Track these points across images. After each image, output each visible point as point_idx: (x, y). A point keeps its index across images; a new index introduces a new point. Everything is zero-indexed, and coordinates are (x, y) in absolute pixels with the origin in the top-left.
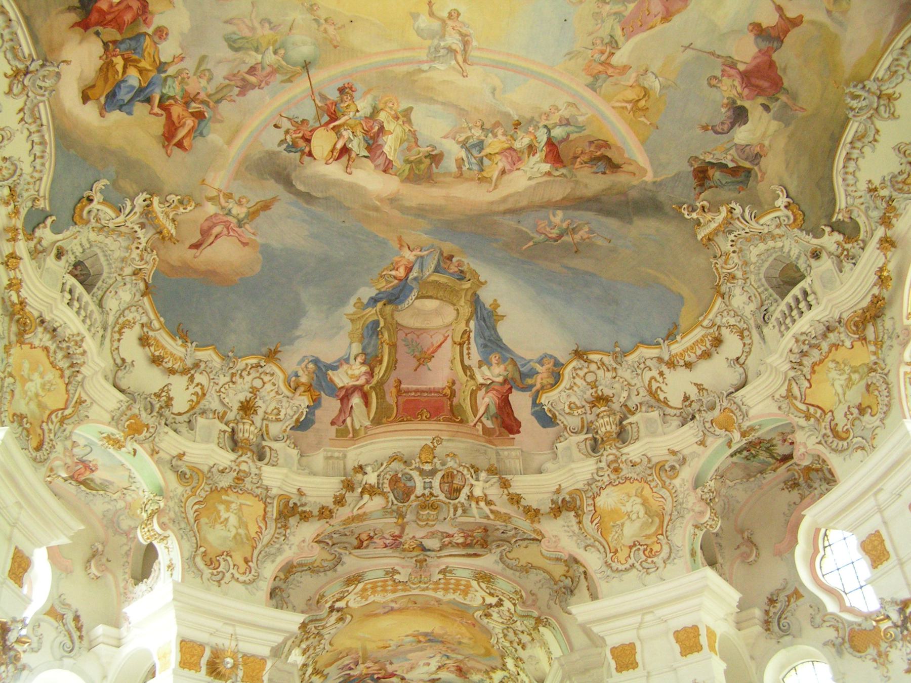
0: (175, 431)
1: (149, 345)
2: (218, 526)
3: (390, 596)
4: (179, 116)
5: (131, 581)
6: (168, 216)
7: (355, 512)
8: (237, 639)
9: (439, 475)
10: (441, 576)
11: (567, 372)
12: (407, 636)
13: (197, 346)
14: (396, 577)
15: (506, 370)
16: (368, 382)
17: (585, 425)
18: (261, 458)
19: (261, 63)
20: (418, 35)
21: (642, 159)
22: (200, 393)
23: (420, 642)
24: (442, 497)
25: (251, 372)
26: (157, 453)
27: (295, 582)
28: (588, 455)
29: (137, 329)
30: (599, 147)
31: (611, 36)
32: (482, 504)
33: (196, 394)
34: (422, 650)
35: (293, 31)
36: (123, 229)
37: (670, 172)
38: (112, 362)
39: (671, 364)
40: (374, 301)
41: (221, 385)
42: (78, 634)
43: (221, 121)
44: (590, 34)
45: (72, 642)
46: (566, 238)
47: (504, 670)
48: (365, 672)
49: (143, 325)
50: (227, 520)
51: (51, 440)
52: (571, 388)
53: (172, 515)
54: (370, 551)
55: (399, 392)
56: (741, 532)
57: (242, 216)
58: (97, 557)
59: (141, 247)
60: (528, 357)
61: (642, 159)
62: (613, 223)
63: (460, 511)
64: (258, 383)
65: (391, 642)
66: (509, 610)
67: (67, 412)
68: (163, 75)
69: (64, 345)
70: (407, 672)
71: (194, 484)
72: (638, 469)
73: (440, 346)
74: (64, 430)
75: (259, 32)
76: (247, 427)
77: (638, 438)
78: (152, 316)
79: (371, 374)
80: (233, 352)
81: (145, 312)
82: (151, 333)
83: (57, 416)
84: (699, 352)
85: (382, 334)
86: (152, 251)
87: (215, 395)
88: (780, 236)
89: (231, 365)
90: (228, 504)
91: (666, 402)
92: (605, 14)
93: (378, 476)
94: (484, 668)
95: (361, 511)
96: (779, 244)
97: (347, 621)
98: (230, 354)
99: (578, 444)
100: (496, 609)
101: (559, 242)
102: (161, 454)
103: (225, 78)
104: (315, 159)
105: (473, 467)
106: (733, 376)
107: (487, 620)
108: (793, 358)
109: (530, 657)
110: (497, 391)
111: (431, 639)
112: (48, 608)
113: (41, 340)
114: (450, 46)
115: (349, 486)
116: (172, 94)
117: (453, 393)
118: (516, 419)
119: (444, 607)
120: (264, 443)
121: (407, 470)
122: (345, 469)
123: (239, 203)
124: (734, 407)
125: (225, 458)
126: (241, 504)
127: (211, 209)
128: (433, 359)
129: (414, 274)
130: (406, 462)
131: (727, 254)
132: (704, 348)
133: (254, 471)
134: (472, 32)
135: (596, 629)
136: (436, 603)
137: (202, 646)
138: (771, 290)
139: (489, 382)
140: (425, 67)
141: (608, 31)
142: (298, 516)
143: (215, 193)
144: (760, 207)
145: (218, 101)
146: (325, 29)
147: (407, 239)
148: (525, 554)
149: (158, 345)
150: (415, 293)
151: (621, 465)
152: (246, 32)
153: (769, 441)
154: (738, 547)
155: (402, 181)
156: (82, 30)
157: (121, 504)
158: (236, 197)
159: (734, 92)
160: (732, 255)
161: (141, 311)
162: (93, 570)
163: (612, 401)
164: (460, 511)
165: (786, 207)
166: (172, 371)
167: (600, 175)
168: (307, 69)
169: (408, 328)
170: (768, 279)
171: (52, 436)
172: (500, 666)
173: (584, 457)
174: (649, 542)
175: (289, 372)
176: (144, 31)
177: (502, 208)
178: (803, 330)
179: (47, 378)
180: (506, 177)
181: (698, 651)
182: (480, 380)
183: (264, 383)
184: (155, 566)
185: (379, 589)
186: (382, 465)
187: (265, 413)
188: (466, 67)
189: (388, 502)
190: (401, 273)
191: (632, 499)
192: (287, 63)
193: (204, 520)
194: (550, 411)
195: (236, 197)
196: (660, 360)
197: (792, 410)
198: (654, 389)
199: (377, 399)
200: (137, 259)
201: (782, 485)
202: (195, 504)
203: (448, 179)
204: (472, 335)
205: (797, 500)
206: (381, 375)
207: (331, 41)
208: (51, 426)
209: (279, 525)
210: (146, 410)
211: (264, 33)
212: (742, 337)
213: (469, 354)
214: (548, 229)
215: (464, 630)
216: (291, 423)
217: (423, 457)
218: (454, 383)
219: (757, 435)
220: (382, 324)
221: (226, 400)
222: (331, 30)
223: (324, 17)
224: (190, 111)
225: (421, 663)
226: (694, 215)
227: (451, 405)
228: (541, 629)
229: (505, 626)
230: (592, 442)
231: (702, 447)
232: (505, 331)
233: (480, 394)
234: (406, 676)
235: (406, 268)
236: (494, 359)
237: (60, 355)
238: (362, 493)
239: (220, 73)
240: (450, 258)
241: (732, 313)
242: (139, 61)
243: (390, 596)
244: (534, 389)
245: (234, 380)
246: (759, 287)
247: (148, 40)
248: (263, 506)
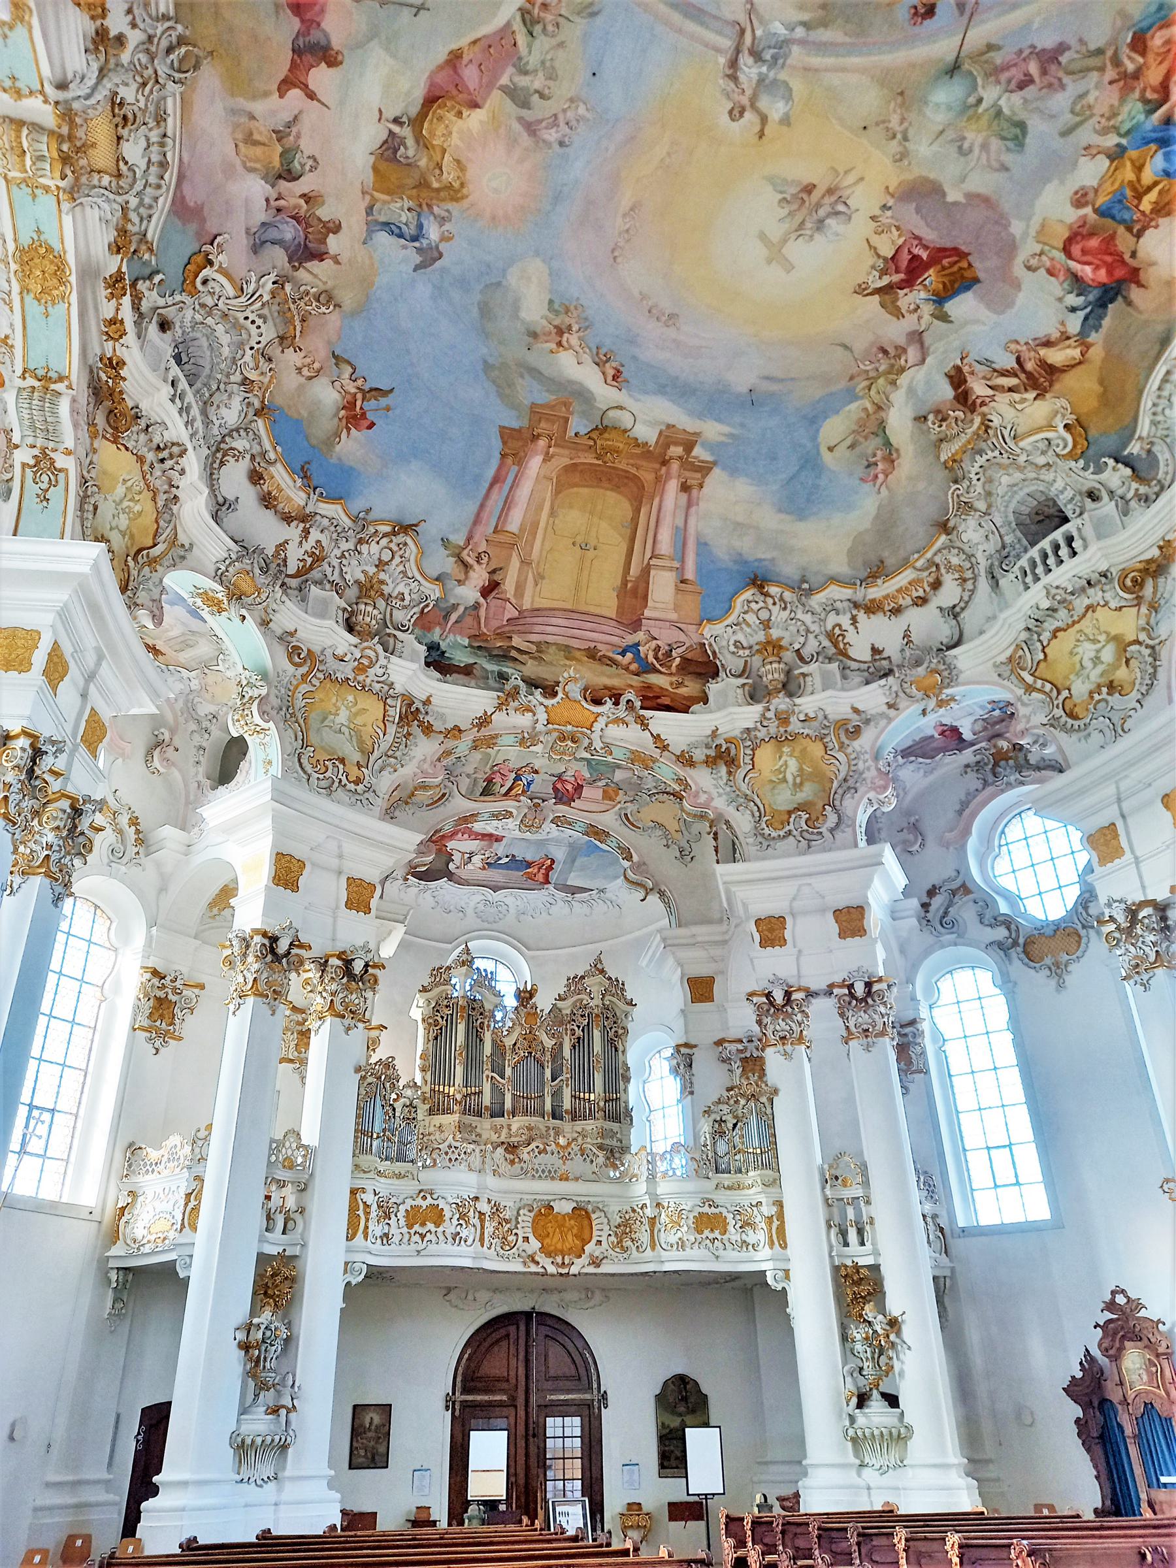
4: (1161, 63)
19: (1007, 91)
20: (791, 90)
31: (531, 34)
35: (941, 128)
43: (1122, 13)
44: (561, 45)
68: (1124, 141)
75: (980, 140)
92: (540, 74)
103: (1063, 87)
114: (756, 62)
116: (1139, 105)
134: (721, 81)
140: (800, 32)
141: (537, 44)
145: (1100, 52)
146: (901, 123)
152: (995, 144)
156: (1142, 273)
168: (956, 62)
176: (1095, 216)
188: (742, 18)
192: (975, 79)
207: (902, 105)
211: (974, 137)
222: (894, 122)
223: (895, 142)
224: (1141, 60)
239: (1061, 101)
242: (1130, 182)
247: (1101, 200)
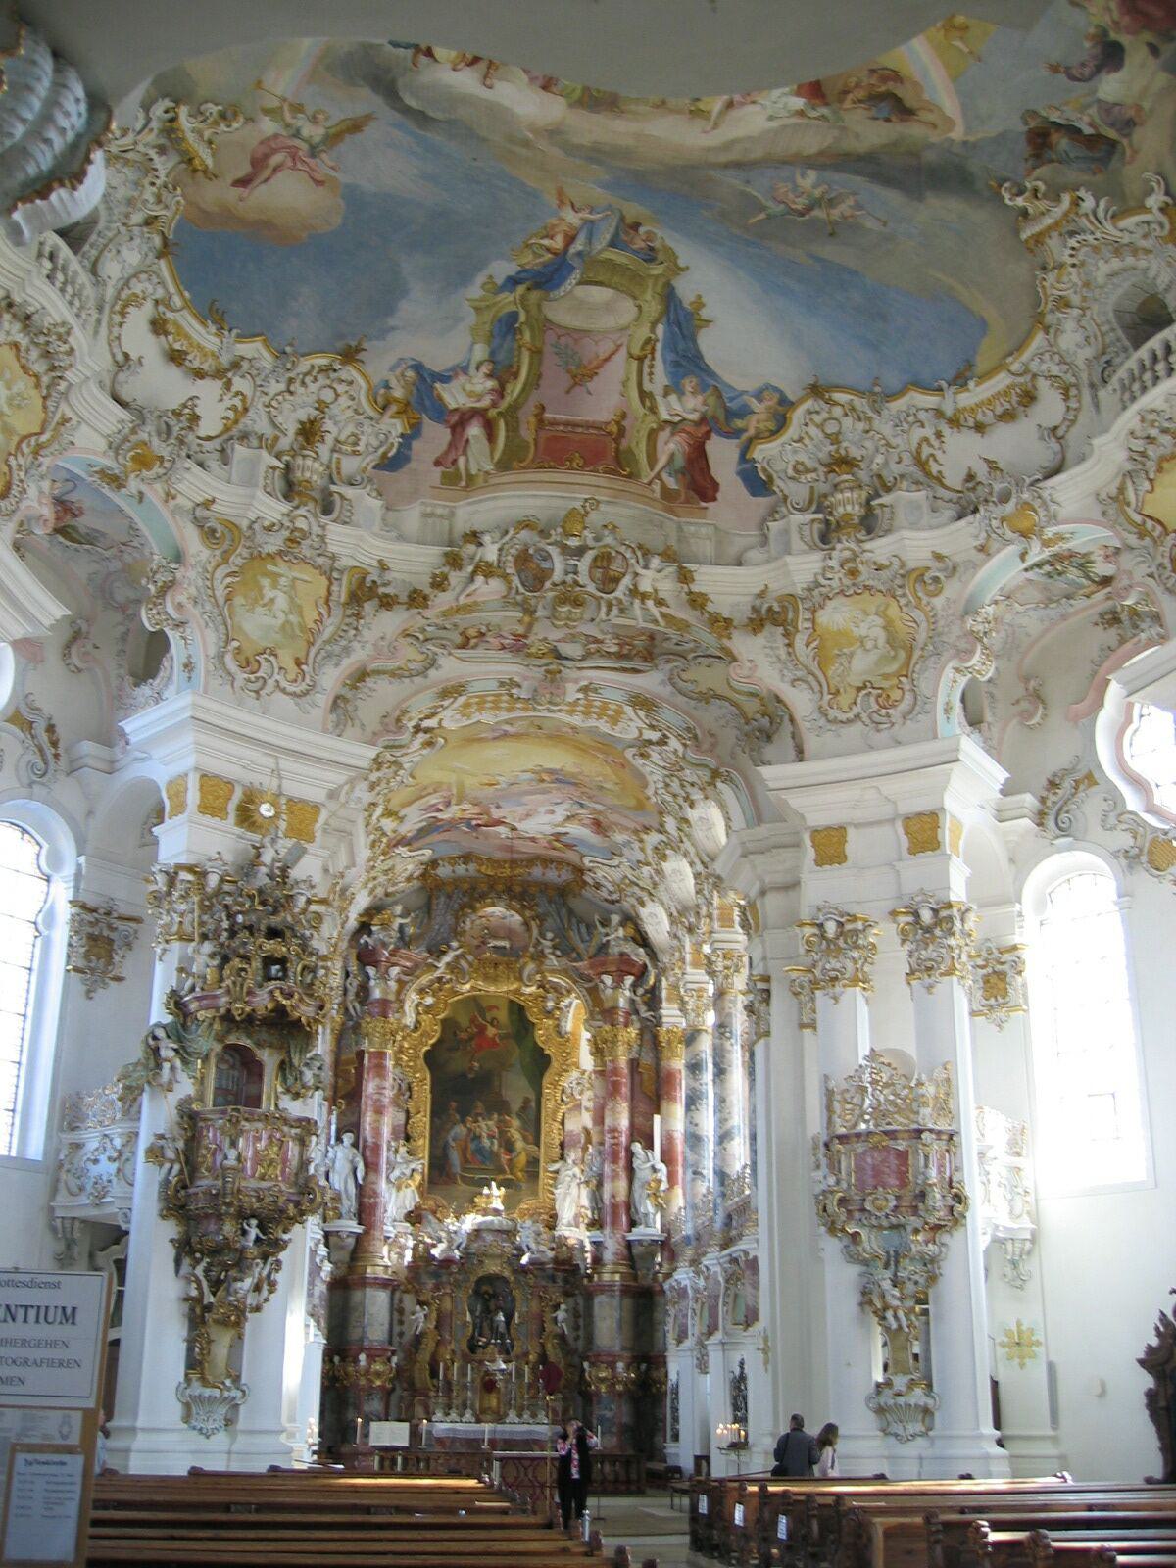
0: (201, 465)
1: (166, 334)
2: (259, 610)
3: (505, 716)
5: (129, 680)
6: (201, 136)
7: (462, 600)
8: (280, 777)
9: (589, 555)
10: (581, 695)
11: (797, 415)
13: (238, 336)
14: (514, 691)
15: (705, 403)
16: (494, 404)
17: (816, 495)
18: (327, 510)
21: (949, 104)
22: (240, 408)
23: (543, 781)
24: (591, 588)
25: (320, 377)
26: (174, 498)
27: (366, 690)
28: (813, 547)
29: (148, 308)
30: (884, 79)
32: (650, 603)
33: (234, 408)
34: (544, 792)
36: (130, 155)
37: (992, 130)
38: (109, 357)
39: (954, 422)
40: (513, 282)
41: (272, 394)
42: (53, 750)
45: (46, 763)
46: (817, 213)
48: (459, 815)
49: (157, 302)
50: (272, 600)
51: (21, 481)
52: (800, 440)
53: (193, 591)
54: (480, 652)
55: (541, 422)
56: (1026, 679)
57: (317, 139)
58: (80, 642)
59: (158, 182)
60: (740, 384)
61: (949, 104)
62: (893, 197)
63: (615, 611)
64: (328, 395)
66: (676, 751)
67: (44, 438)
69: (42, 339)
70: (521, 820)
71: (226, 546)
72: (885, 574)
73: (607, 359)
74: (40, 466)
76: (309, 462)
77: (888, 532)
78: (172, 288)
79: (500, 392)
80: (291, 345)
81: (162, 283)
82: (169, 315)
83: (29, 445)
84: (999, 410)
85: (521, 333)
86: (175, 189)
87: (262, 411)
88: (1148, 251)
89: (289, 366)
90: (275, 577)
91: (939, 480)
93: (500, 550)
94: (632, 825)
95: (469, 600)
96: (1142, 263)
97: (438, 746)
98: (288, 349)
99: (800, 527)
100: (657, 748)
101: (807, 217)
102: (180, 500)
104: (436, 60)
105: (640, 547)
106: (1044, 453)
107: (641, 761)
108: (1138, 445)
109: (701, 818)
110: (688, 433)
111: (559, 778)
112: (10, 713)
113: (8, 333)
115: (454, 561)
117: (622, 432)
118: (712, 479)
119: (579, 737)
120: (333, 488)
121: (542, 544)
122: (450, 531)
123: (314, 120)
124: (1036, 503)
125: (274, 509)
126: (295, 579)
127: (268, 126)
128: (595, 378)
129: (578, 246)
130: (542, 532)
131: (1061, 266)
132: (1007, 405)
133: (316, 530)
135: (795, 801)
137: (230, 784)
138: (1120, 333)
139: (677, 419)
142: (376, 601)
143: (276, 103)
144: (1125, 205)
147: (571, 193)
148: (706, 677)
149: (181, 333)
150: (576, 275)
151: (861, 568)
153: (1085, 555)
154: (1018, 701)
155: (571, 106)
157: (115, 565)
158: (310, 110)
159: (1108, 18)
160: (1071, 269)
161: (155, 280)
162: (75, 659)
163: (857, 466)
164: (615, 611)
165: (1162, 210)
166: (199, 374)
167: (880, 122)
169: (559, 326)
170: (1118, 313)
171: (22, 475)
172: (657, 826)
173: (806, 547)
174: (885, 684)
175: (376, 380)
177: (723, 158)
178: (1153, 406)
179: (15, 390)
180: (735, 113)
181: (933, 850)
182: (665, 416)
183: (337, 395)
184: (166, 663)
186: (507, 532)
187: (337, 441)
189: (510, 588)
190: (558, 243)
191: (872, 618)
193: (239, 600)
194: (765, 470)
195: (310, 110)
196: (939, 413)
197: (1122, 519)
198: (924, 456)
199: (507, 431)
200: (152, 199)
201: (1096, 618)
202: (229, 575)
203: (642, 108)
204: (659, 346)
205: (1113, 642)
206: (515, 395)
208: (21, 461)
209: (349, 612)
210: (159, 434)
212: (1066, 397)
213: (651, 374)
214: (791, 196)
215: (608, 770)
216: (373, 459)
217: (568, 526)
218: (624, 416)
219: (1066, 546)
220: (523, 318)
221: (280, 420)
225: (543, 809)
226: (1020, 201)
227: (617, 450)
228: (720, 785)
230: (822, 526)
231: (981, 556)
232: (710, 345)
233: (664, 436)
235: (566, 235)
236: (689, 384)
237: (35, 354)
238: (474, 573)
240: (636, 226)
241: (1057, 358)
243: (505, 716)
244: (745, 436)
245: (292, 388)
246: (1103, 324)
248: (324, 581)
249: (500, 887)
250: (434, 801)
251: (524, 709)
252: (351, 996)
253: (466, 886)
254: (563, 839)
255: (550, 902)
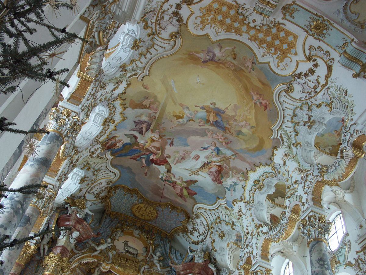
3: (224, 35)
12: (203, 108)
23: (208, 121)
34: (203, 134)
47: (267, 164)
65: (187, 112)
70: (178, 162)
136: (250, 66)
185: (220, 17)
215: (252, 116)
229: (298, 104)
234: (174, 169)
249: (138, 225)
250: (144, 118)
251: (238, 32)
252: (45, 241)
253: (121, 219)
254: (192, 187)
255: (161, 240)
